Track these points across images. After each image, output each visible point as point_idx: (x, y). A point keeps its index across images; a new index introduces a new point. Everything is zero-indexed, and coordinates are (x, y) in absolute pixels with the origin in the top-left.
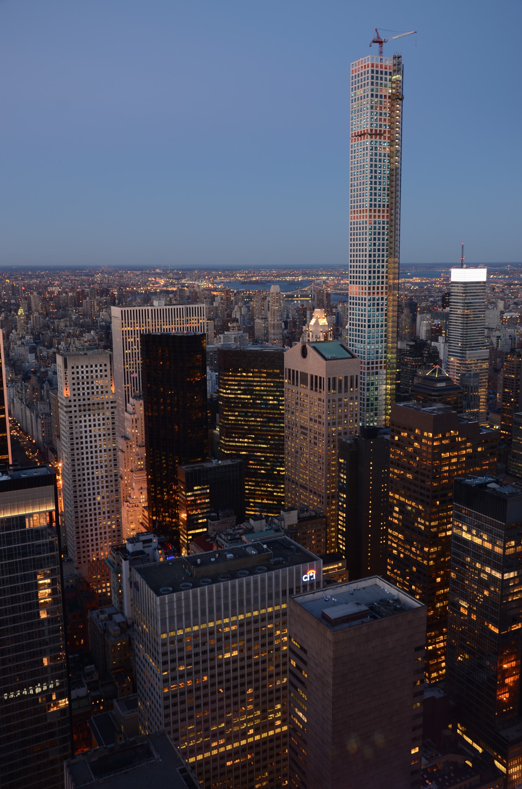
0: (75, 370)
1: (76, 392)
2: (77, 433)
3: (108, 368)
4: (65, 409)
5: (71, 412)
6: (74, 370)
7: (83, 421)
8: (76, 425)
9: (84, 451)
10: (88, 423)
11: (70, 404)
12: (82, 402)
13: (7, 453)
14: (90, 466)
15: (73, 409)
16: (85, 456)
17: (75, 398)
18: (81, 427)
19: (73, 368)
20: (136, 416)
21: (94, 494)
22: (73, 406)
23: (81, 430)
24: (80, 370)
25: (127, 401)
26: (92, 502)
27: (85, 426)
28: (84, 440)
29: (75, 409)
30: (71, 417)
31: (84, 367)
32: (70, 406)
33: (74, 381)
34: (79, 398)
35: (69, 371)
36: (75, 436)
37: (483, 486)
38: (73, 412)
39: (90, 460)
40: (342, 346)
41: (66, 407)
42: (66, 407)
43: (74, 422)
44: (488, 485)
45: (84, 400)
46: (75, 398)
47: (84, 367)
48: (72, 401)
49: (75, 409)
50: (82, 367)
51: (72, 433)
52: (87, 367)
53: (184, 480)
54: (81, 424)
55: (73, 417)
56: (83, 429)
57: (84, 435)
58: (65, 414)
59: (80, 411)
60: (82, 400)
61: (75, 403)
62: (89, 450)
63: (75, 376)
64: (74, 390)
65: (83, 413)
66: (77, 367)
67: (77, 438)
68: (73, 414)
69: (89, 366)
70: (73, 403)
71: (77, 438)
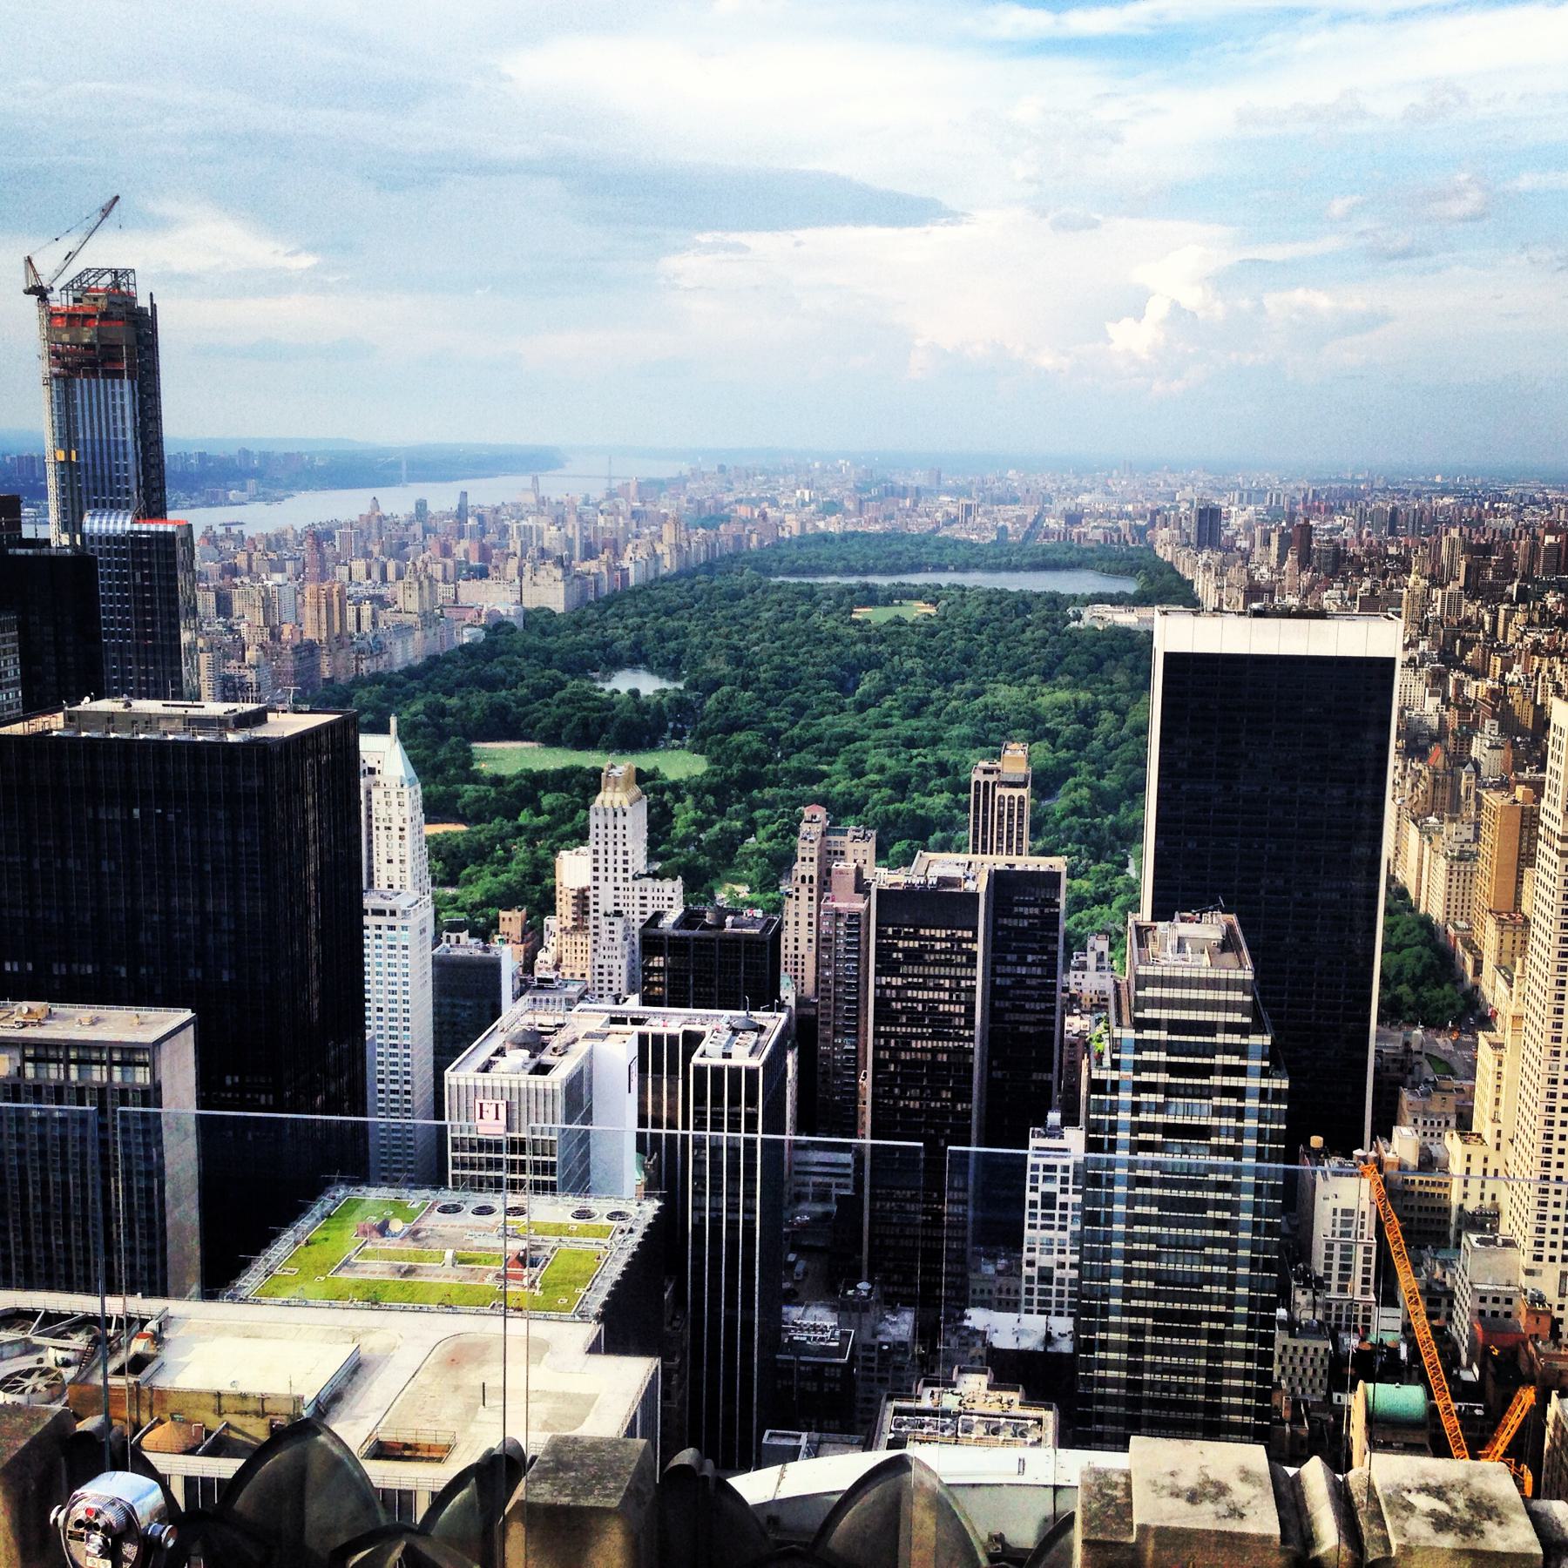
4: (1558, 845)
58: (1556, 858)
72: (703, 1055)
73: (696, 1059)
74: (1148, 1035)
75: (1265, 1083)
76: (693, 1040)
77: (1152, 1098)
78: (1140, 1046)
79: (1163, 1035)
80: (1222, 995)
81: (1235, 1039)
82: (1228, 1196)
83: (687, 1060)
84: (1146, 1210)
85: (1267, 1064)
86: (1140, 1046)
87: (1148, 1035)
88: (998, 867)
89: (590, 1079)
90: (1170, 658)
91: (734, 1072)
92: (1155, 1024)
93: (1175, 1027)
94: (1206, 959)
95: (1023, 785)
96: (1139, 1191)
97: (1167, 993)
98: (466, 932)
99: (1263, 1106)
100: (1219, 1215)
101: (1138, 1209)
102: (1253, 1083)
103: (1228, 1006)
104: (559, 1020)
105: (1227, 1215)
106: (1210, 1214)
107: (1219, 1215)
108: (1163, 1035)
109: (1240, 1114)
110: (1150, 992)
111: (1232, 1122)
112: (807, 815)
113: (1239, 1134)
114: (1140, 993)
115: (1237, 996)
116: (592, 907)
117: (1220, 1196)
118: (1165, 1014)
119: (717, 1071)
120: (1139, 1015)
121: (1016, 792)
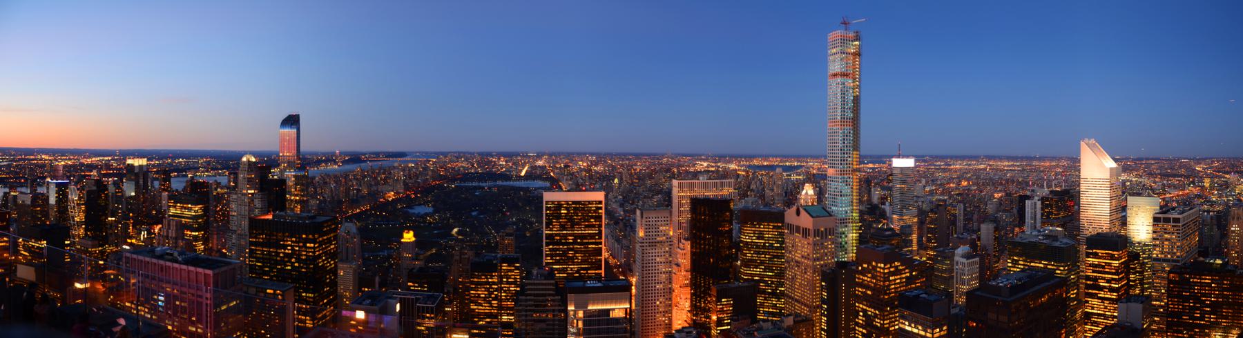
1: (647, 234)
3: (668, 219)
6: (647, 220)
12: (651, 241)
13: (601, 269)
14: (653, 281)
16: (651, 275)
20: (685, 251)
25: (679, 241)
35: (644, 219)
36: (645, 262)
37: (918, 296)
40: (823, 208)
41: (641, 243)
42: (641, 243)
44: (921, 296)
53: (715, 294)
56: (651, 258)
57: (651, 262)
62: (654, 271)
68: (645, 248)
74: (528, 298)
75: (560, 308)
77: (530, 313)
78: (526, 300)
79: (532, 298)
80: (547, 287)
86: (526, 300)
87: (528, 298)
92: (530, 295)
93: (535, 295)
94: (543, 278)
97: (533, 287)
102: (557, 308)
103: (549, 290)
108: (532, 298)
110: (528, 287)
115: (552, 287)
118: (533, 292)
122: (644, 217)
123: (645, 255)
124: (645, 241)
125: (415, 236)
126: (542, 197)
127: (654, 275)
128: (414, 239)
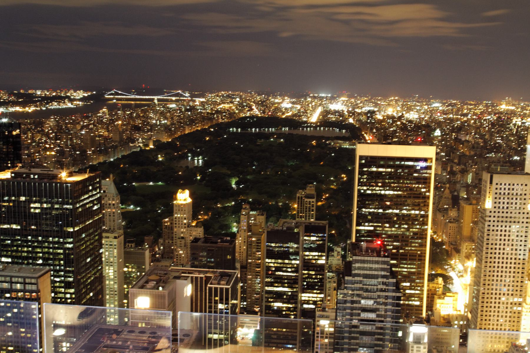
0: (499, 186)
1: (497, 205)
2: (492, 240)
5: (490, 221)
6: (497, 186)
7: (499, 231)
8: (493, 233)
9: (497, 256)
10: (503, 233)
11: (490, 214)
12: (501, 214)
14: (500, 269)
15: (492, 219)
16: (497, 260)
17: (495, 210)
18: (497, 235)
19: (497, 184)
21: (500, 294)
22: (492, 216)
23: (496, 237)
24: (503, 187)
26: (497, 301)
27: (501, 235)
28: (498, 247)
29: (494, 219)
30: (489, 226)
31: (507, 184)
32: (490, 216)
33: (496, 196)
34: (499, 210)
35: (494, 186)
36: (490, 242)
38: (492, 221)
39: (500, 265)
43: (491, 230)
45: (503, 212)
46: (495, 210)
47: (507, 184)
48: (493, 212)
49: (494, 219)
50: (505, 184)
51: (488, 239)
52: (509, 185)
54: (497, 233)
55: (491, 226)
56: (499, 238)
57: (498, 242)
59: (498, 221)
60: (501, 212)
61: (495, 214)
63: (498, 191)
64: (495, 203)
65: (500, 224)
66: (501, 184)
67: (492, 244)
68: (491, 224)
69: (511, 185)
70: (492, 214)
71: (492, 244)
72: (211, 284)
73: (209, 285)
75: (394, 294)
76: (208, 279)
81: (385, 280)
82: (382, 331)
83: (206, 286)
84: (355, 335)
85: (394, 288)
87: (357, 279)
88: (306, 224)
89: (175, 291)
90: (361, 158)
91: (222, 289)
92: (358, 275)
93: (366, 276)
94: (375, 254)
95: (313, 198)
96: (353, 329)
98: (134, 243)
99: (393, 301)
100: (379, 337)
101: (353, 335)
104: (165, 272)
105: (381, 337)
106: (376, 336)
107: (379, 337)
108: (361, 279)
109: (386, 304)
111: (383, 307)
112: (244, 206)
113: (386, 311)
114: (353, 265)
116: (174, 236)
117: (379, 331)
118: (362, 272)
119: (216, 289)
120: (353, 272)
121: (311, 200)
122: (494, 182)
123: (491, 233)
124: (492, 214)
125: (191, 196)
126: (354, 150)
127: (501, 260)
128: (189, 200)
